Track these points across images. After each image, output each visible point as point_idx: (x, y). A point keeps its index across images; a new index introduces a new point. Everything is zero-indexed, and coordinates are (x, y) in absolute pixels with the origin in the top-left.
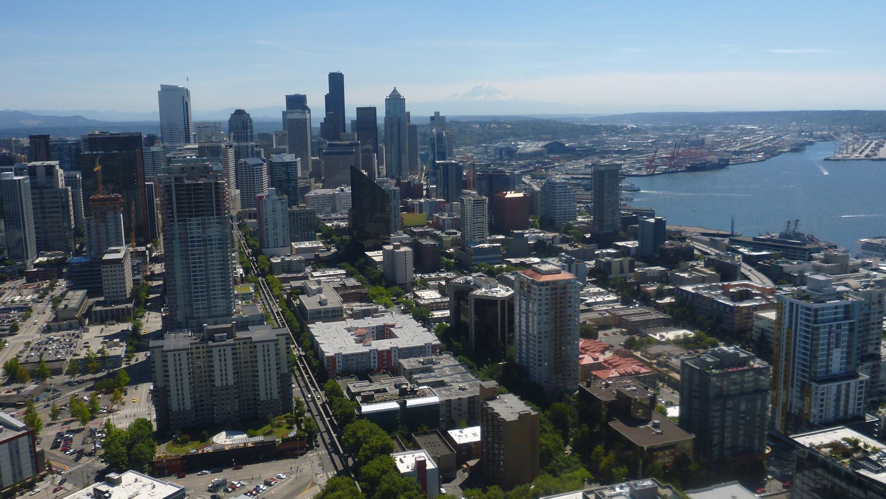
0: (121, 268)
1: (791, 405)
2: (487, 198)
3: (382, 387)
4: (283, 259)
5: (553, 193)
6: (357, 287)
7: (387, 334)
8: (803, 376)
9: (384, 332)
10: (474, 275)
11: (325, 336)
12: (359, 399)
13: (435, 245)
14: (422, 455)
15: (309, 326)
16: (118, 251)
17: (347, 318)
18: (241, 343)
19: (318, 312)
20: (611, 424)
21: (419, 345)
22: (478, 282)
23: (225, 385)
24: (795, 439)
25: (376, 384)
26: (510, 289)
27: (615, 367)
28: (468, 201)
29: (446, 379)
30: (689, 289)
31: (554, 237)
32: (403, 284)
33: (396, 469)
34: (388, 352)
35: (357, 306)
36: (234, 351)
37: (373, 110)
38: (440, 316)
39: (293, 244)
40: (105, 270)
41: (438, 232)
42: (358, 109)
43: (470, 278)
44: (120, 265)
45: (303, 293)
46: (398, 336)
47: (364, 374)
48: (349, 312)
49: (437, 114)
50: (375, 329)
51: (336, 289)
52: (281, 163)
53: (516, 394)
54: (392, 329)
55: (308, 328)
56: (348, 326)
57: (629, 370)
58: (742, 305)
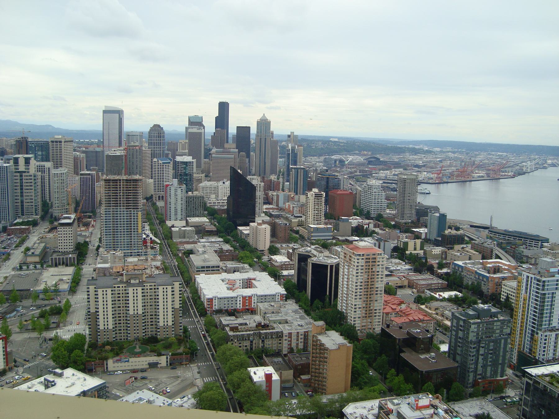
0: (70, 229)
1: (524, 346)
3: (244, 322)
7: (250, 284)
8: (533, 327)
10: (313, 247)
11: (206, 284)
13: (286, 224)
14: (270, 370)
16: (69, 218)
18: (149, 286)
19: (203, 267)
20: (402, 355)
21: (271, 293)
22: (315, 253)
23: (136, 313)
24: (526, 370)
25: (240, 319)
27: (407, 315)
28: (311, 195)
29: (289, 318)
30: (460, 263)
32: (263, 251)
33: (251, 378)
34: (250, 297)
35: (230, 264)
36: (143, 291)
37: (249, 128)
39: (188, 218)
40: (60, 230)
41: (289, 216)
43: (309, 249)
44: (70, 227)
46: (257, 286)
47: (232, 313)
49: (292, 133)
50: (241, 281)
51: (216, 251)
52: (182, 162)
53: (337, 331)
54: (253, 281)
56: (223, 278)
57: (416, 318)
58: (495, 276)
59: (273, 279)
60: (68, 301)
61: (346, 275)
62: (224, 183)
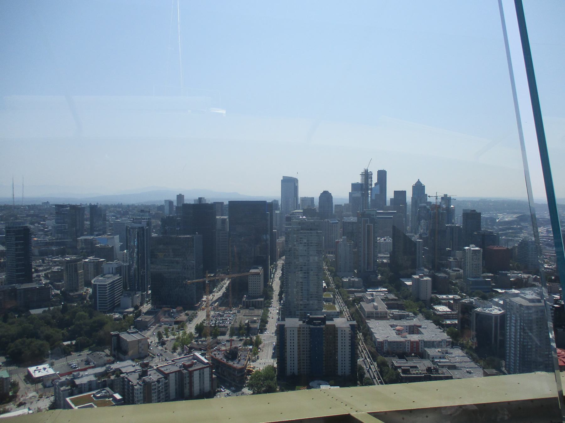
0: (259, 278)
2: (482, 249)
3: (415, 365)
4: (349, 280)
5: (527, 248)
6: (395, 300)
9: (414, 330)
12: (400, 370)
15: (367, 321)
17: (390, 319)
19: (372, 313)
26: (501, 309)
29: (457, 365)
31: (529, 277)
32: (425, 301)
34: (417, 343)
35: (396, 312)
37: (405, 192)
38: (450, 323)
40: (250, 278)
42: (394, 191)
43: (471, 300)
45: (363, 301)
47: (402, 356)
48: (391, 315)
49: (446, 195)
50: (408, 327)
51: (382, 300)
52: (349, 222)
54: (419, 329)
55: (366, 323)
56: (392, 323)
59: (438, 327)
60: (258, 337)
61: (513, 326)
62: (385, 240)
